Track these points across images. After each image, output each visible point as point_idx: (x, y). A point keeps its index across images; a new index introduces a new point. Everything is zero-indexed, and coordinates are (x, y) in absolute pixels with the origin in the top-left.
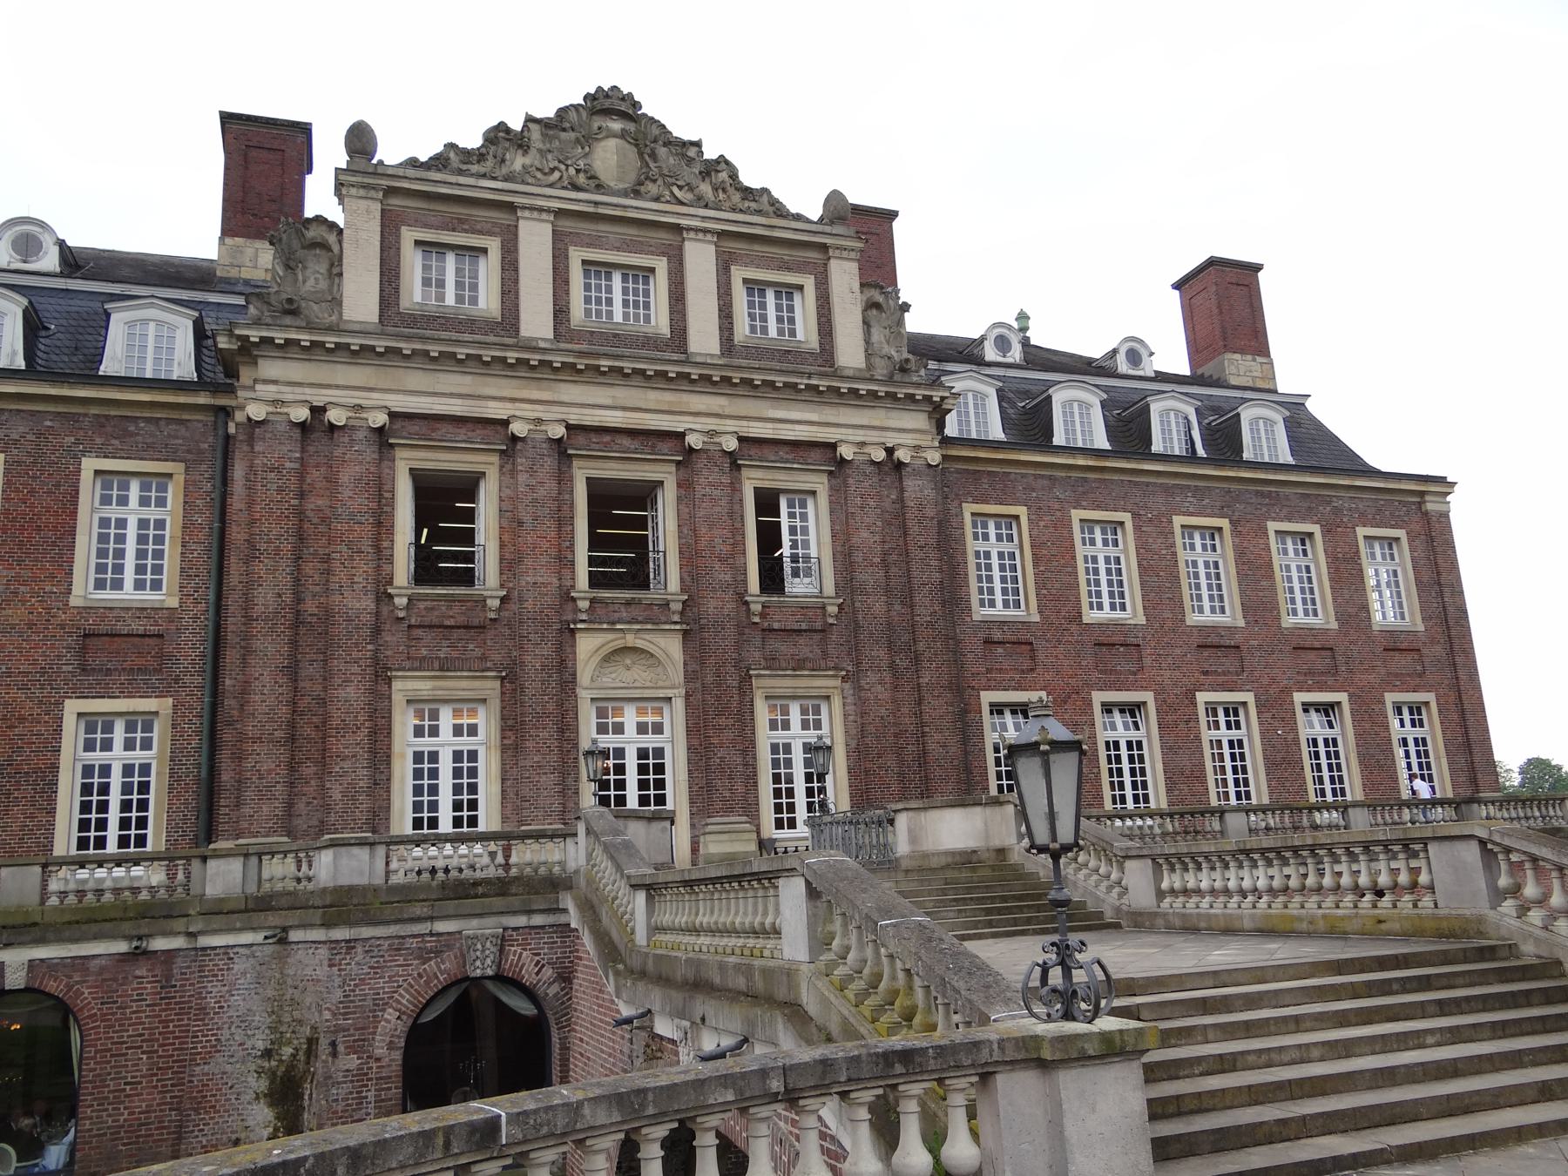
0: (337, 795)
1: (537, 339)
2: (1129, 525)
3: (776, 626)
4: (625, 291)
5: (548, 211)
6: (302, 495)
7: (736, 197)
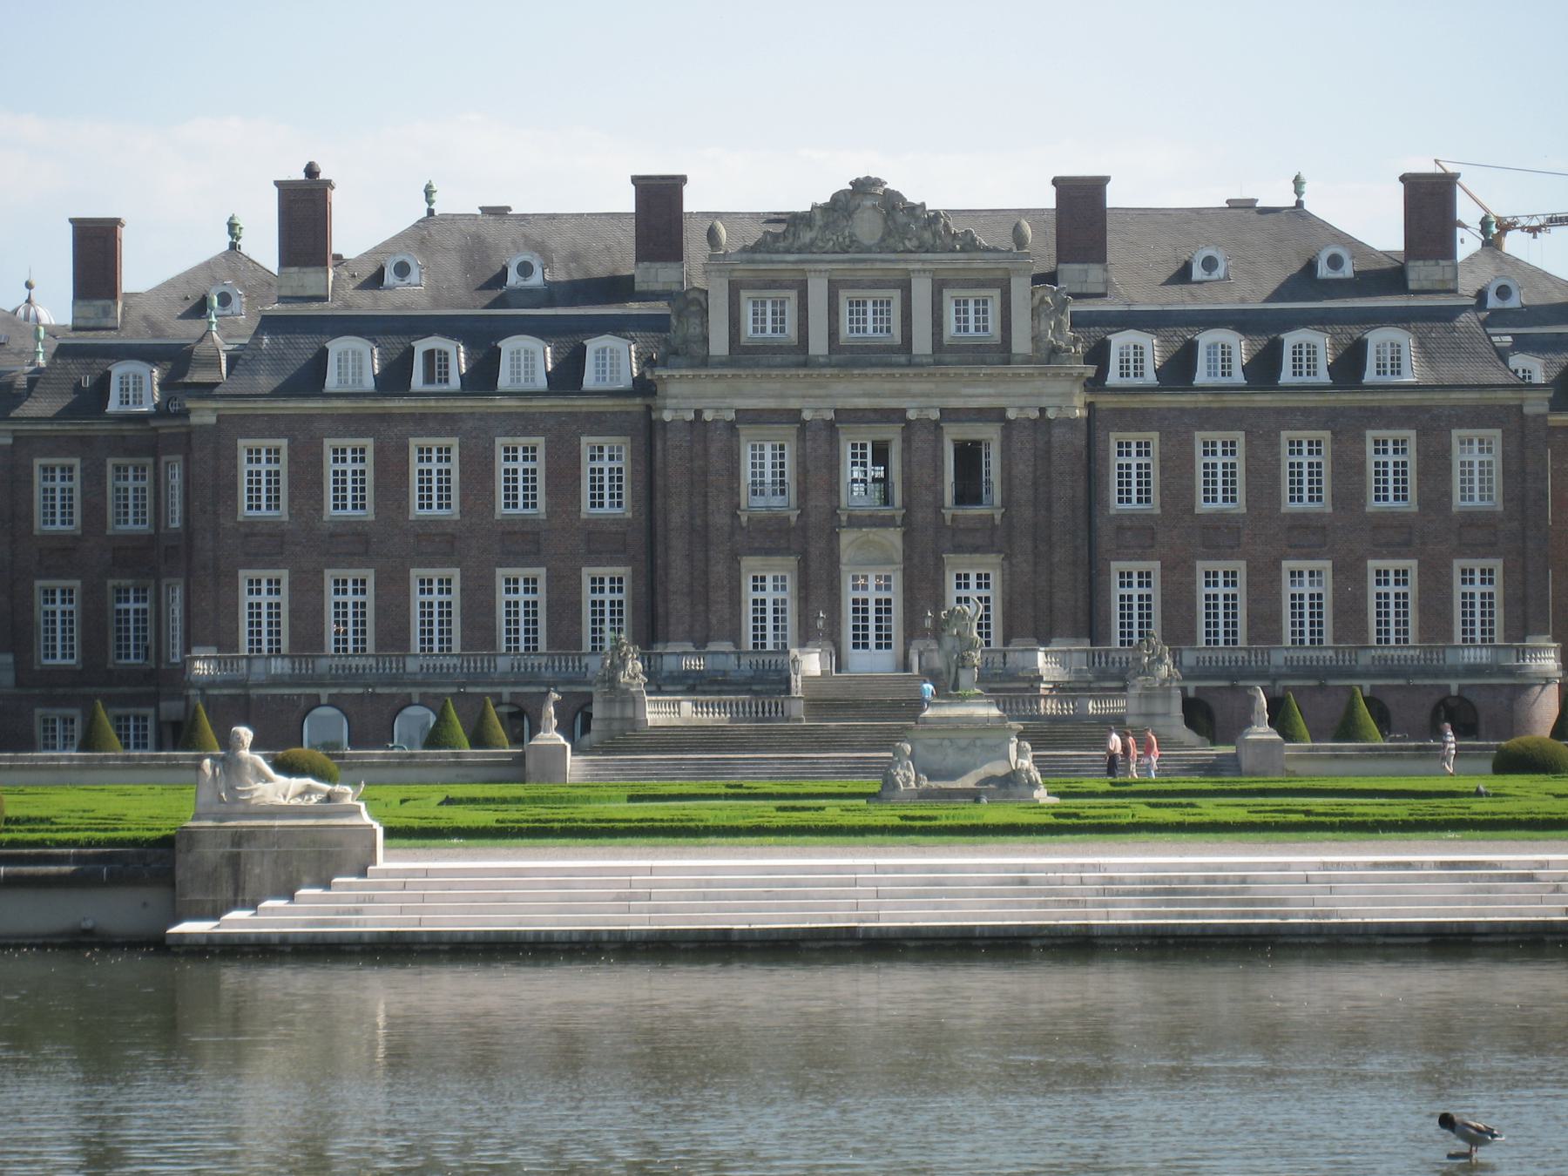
0: (714, 621)
2: (1242, 440)
4: (875, 313)
6: (691, 460)
7: (948, 240)
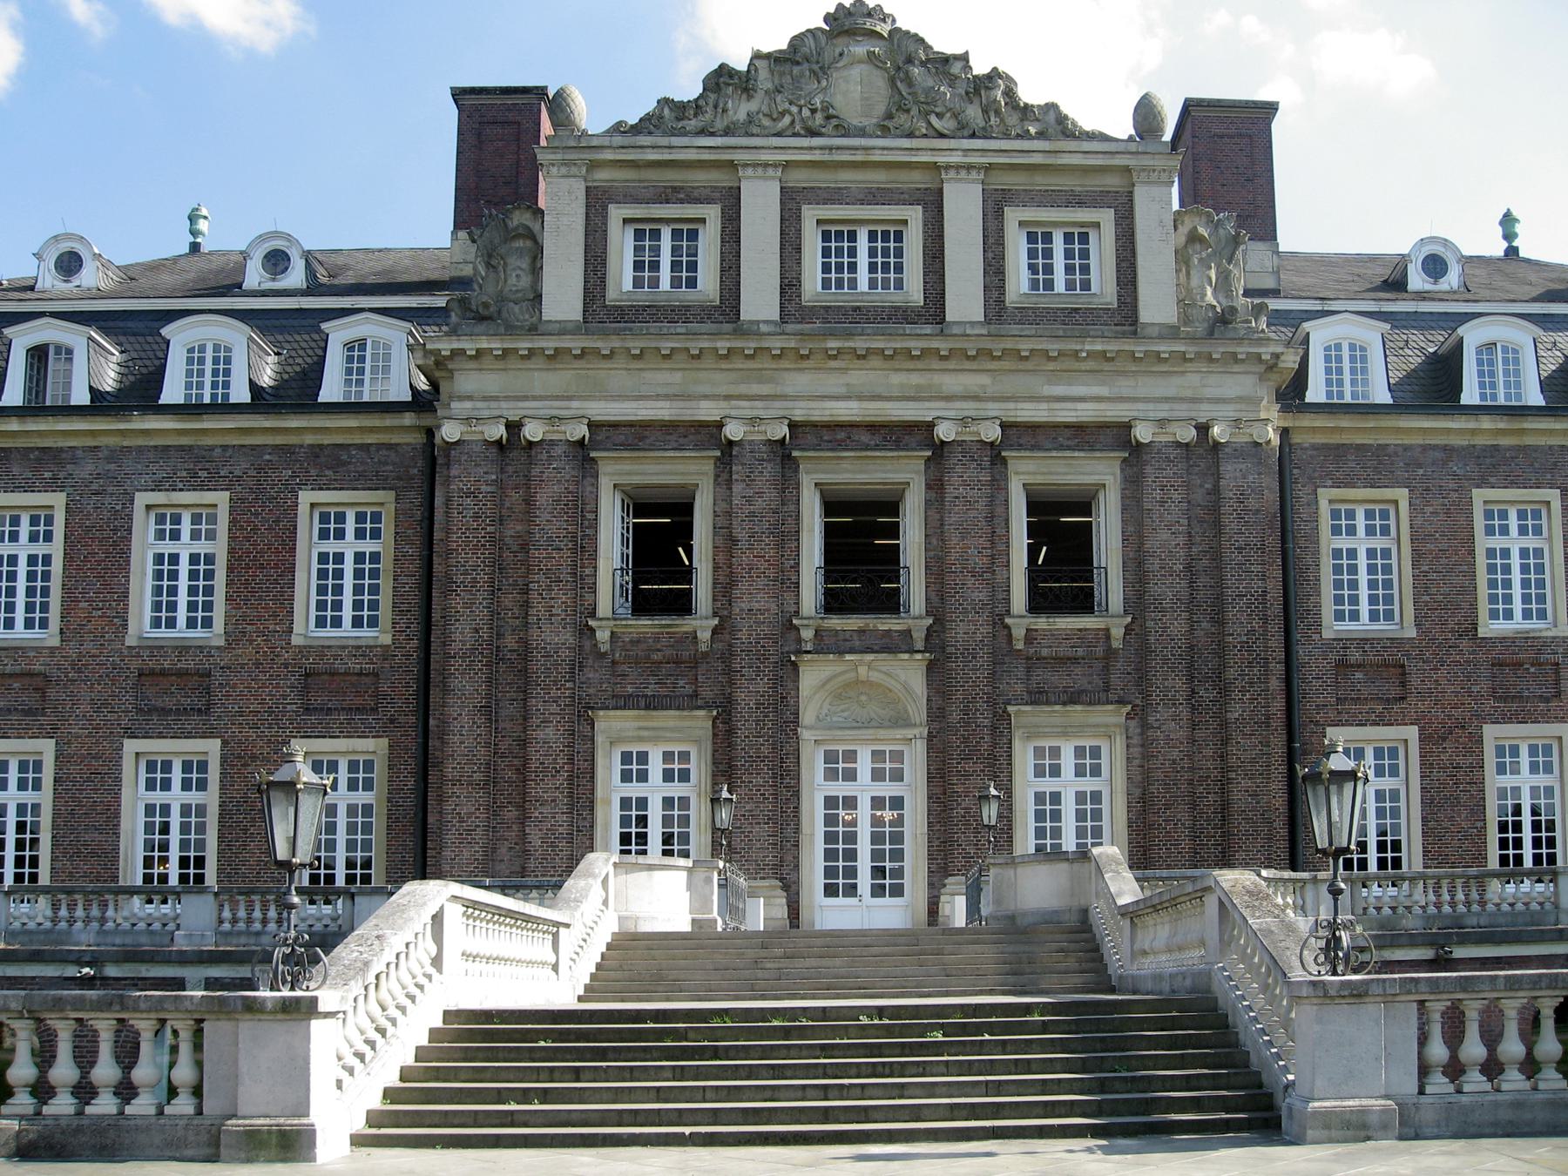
1: (758, 322)
3: (1045, 652)
5: (775, 165)
